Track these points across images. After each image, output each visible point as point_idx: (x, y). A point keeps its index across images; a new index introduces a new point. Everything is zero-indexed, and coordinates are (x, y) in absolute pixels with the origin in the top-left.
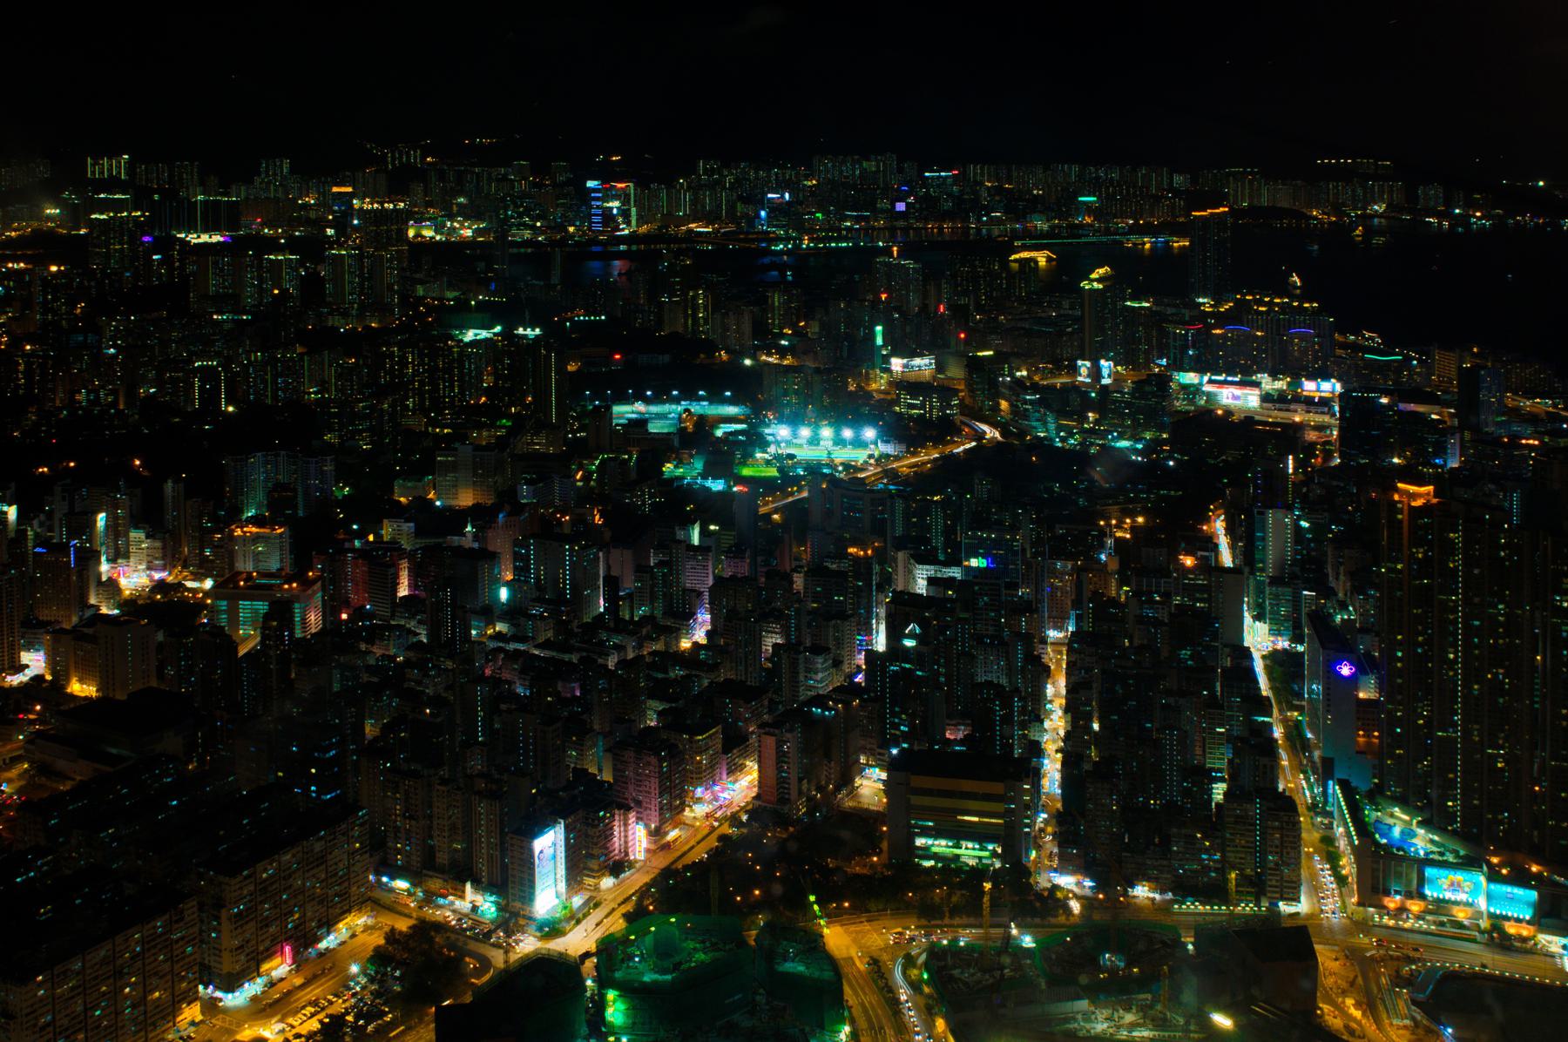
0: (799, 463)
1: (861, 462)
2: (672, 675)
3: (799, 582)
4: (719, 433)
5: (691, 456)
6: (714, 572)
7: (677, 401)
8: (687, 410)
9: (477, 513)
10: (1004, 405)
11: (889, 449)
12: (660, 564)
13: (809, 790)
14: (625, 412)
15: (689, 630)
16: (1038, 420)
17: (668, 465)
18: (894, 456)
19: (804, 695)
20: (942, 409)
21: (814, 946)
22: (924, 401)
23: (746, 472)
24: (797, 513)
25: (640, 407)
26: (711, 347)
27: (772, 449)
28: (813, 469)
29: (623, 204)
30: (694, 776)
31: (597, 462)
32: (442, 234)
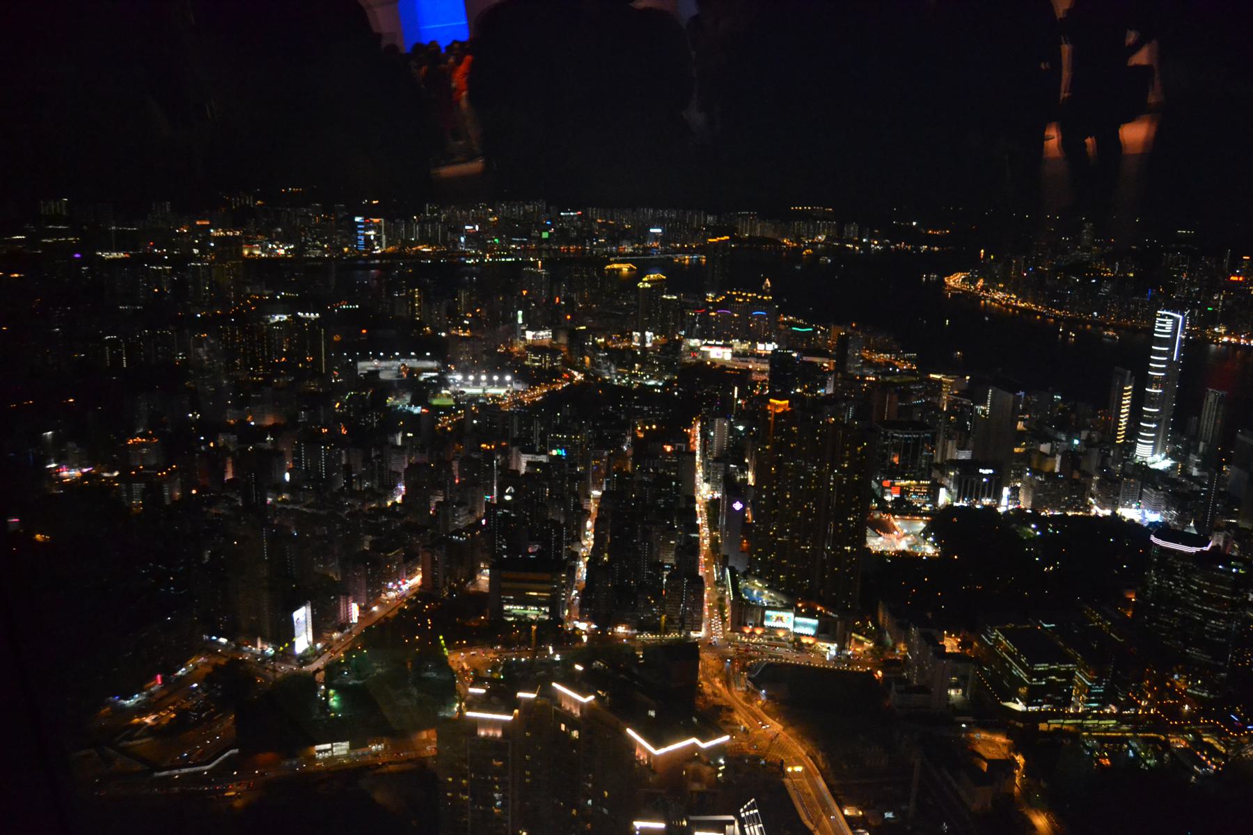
0: (467, 396)
1: (502, 394)
2: (380, 521)
3: (455, 465)
4: (422, 379)
5: (404, 393)
6: (409, 461)
7: (398, 358)
8: (403, 365)
9: (273, 430)
10: (587, 359)
11: (520, 387)
12: (377, 457)
13: (450, 583)
14: (365, 366)
15: (393, 495)
16: (606, 369)
17: (390, 398)
18: (522, 392)
19: (451, 529)
20: (551, 362)
21: (443, 664)
22: (541, 358)
23: (435, 402)
24: (459, 425)
25: (376, 363)
26: (421, 325)
27: (452, 388)
28: (474, 398)
29: (378, 233)
30: (388, 576)
31: (347, 397)
32: (265, 252)
